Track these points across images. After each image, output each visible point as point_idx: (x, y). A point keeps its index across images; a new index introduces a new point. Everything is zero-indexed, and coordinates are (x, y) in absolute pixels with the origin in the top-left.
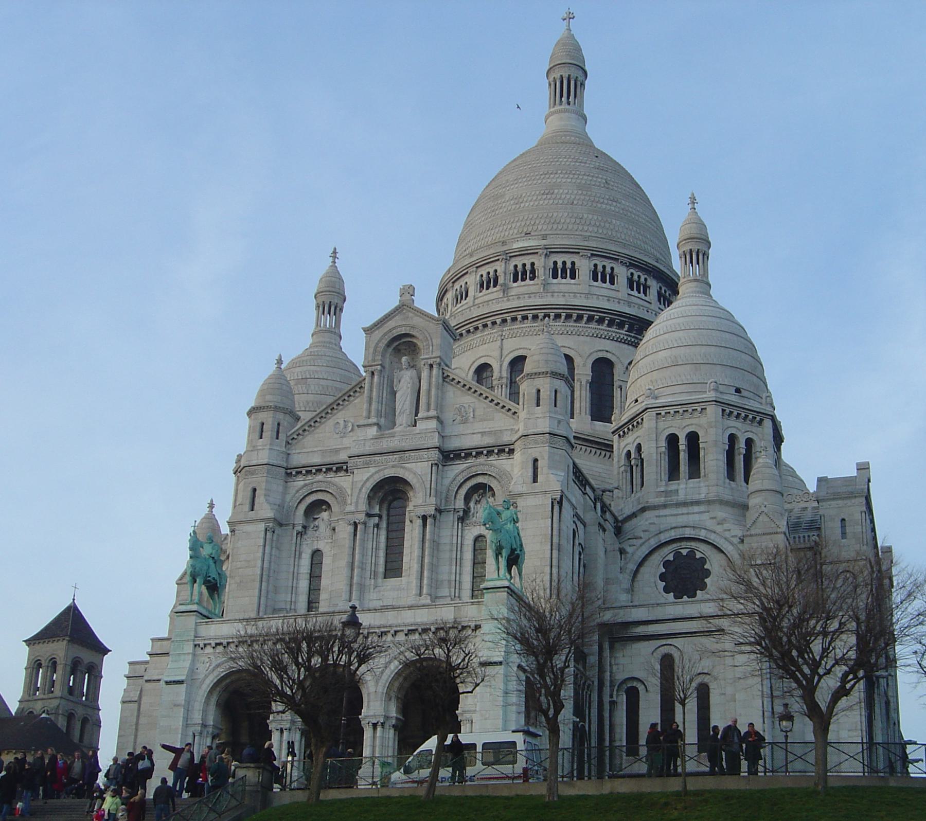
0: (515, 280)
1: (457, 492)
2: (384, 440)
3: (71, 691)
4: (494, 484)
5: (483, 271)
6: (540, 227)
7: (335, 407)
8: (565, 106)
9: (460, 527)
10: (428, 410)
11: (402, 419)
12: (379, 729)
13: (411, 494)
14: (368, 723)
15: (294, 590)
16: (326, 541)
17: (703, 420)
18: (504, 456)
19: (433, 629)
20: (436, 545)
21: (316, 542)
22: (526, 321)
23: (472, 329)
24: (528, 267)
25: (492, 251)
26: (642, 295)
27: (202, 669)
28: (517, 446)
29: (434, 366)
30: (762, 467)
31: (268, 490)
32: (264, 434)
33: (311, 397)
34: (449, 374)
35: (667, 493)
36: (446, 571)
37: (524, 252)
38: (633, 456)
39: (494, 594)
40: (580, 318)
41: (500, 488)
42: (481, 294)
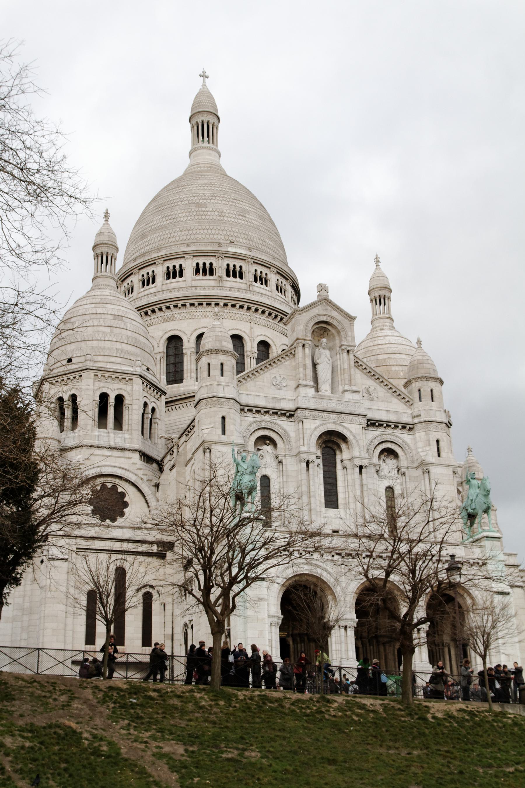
0: (228, 275)
2: (325, 401)
5: (201, 260)
6: (241, 240)
7: (272, 364)
8: (211, 145)
11: (325, 387)
13: (343, 446)
18: (405, 431)
22: (241, 309)
23: (196, 304)
24: (238, 269)
25: (209, 248)
28: (416, 426)
29: (350, 353)
32: (224, 373)
37: (236, 256)
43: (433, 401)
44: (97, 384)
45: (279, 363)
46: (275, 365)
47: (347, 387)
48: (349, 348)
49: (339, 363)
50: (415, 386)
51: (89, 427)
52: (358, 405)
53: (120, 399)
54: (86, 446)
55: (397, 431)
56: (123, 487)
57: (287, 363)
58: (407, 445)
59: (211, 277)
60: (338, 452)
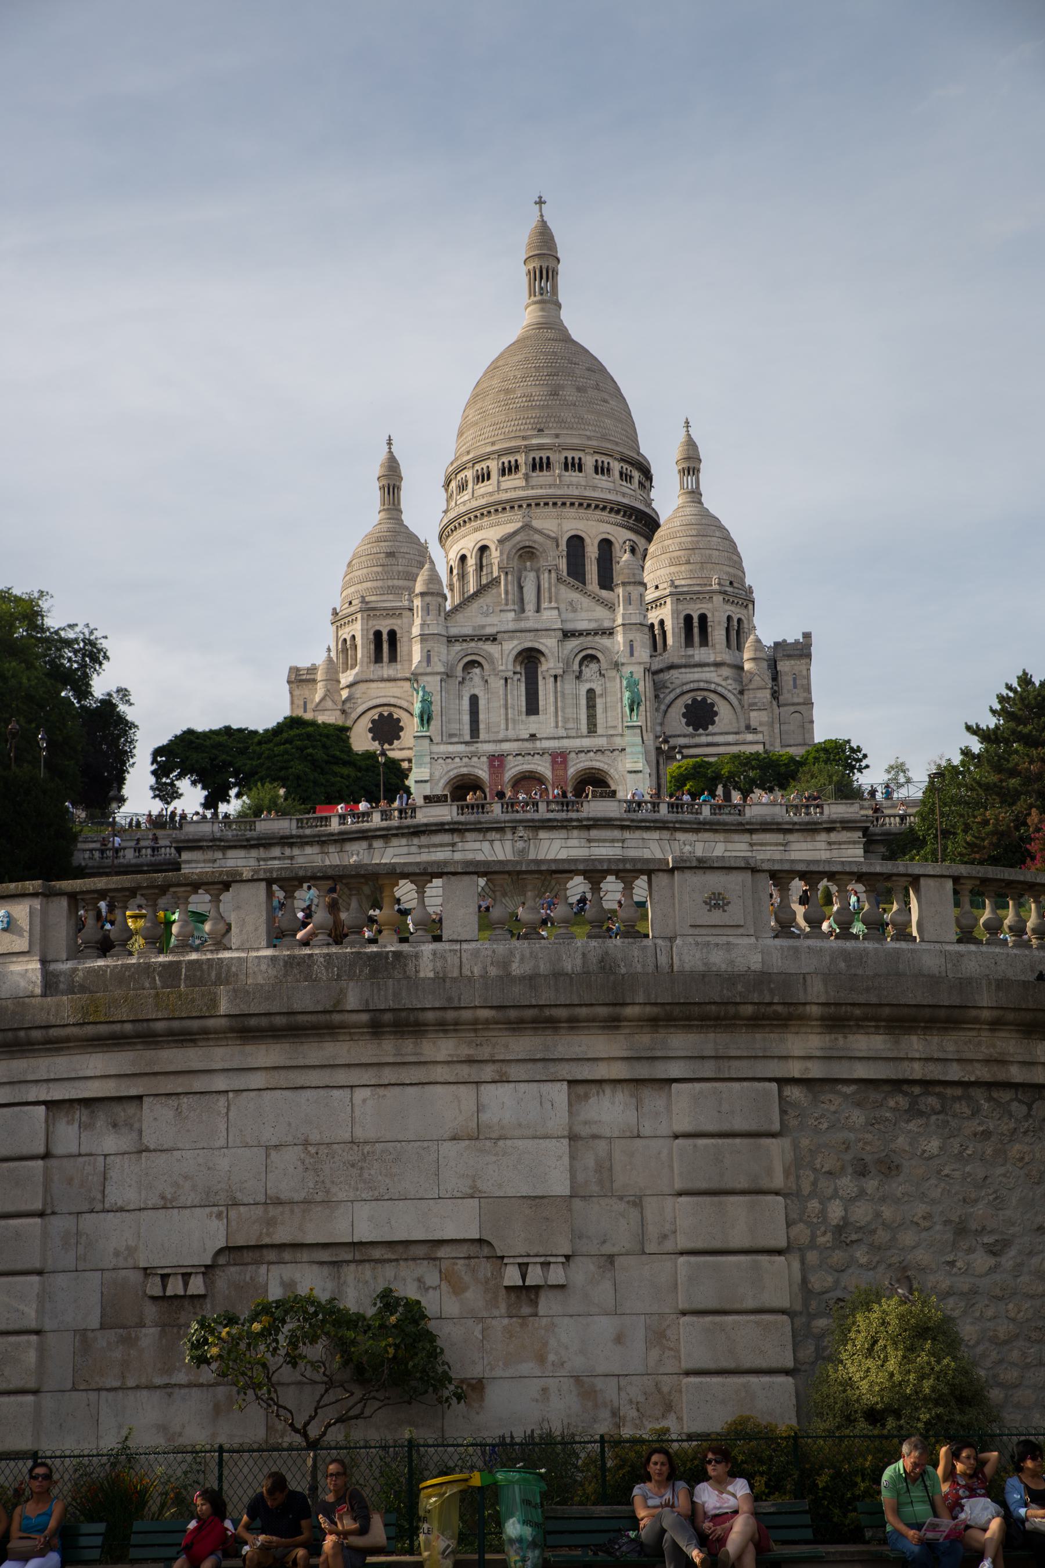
0: (534, 468)
4: (599, 655)
5: (505, 459)
10: (550, 602)
11: (530, 606)
13: (542, 659)
15: (460, 721)
17: (710, 606)
18: (605, 636)
20: (563, 694)
24: (545, 460)
25: (513, 444)
26: (629, 485)
27: (437, 774)
33: (400, 568)
35: (685, 656)
36: (570, 712)
37: (540, 447)
38: (656, 627)
40: (589, 505)
42: (504, 479)
44: (370, 622)
51: (365, 664)
53: (392, 634)
54: (362, 681)
56: (398, 714)
57: (494, 591)
58: (607, 648)
59: (517, 476)
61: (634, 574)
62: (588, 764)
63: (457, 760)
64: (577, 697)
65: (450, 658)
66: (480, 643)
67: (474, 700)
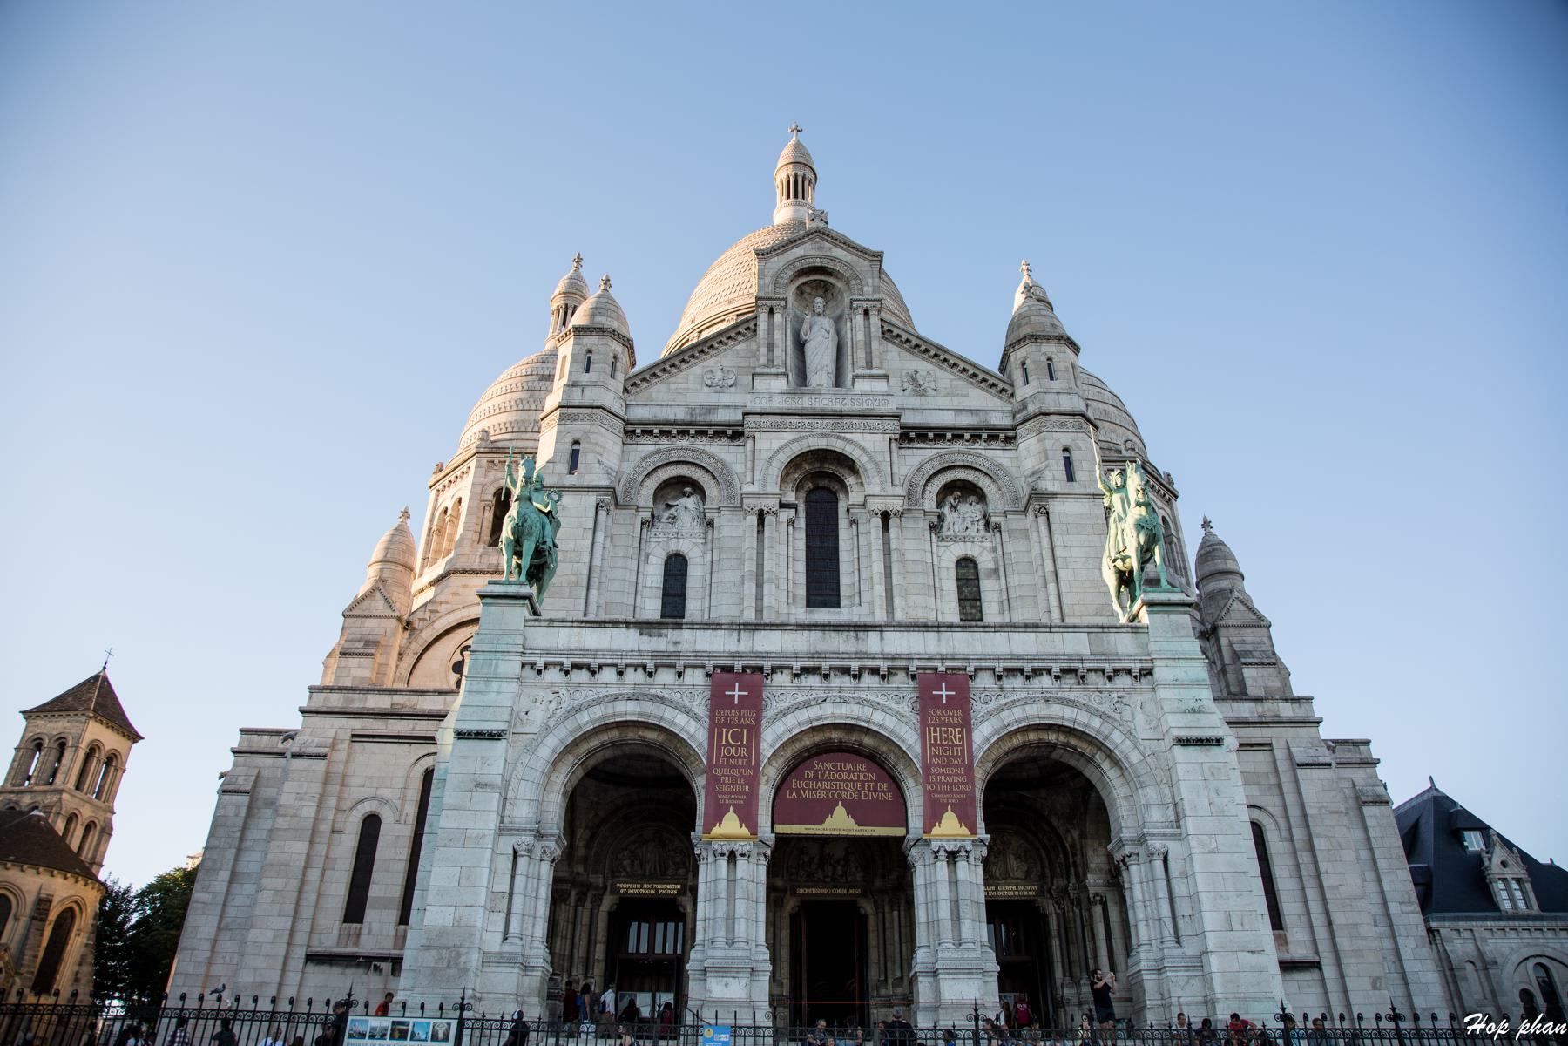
1: (924, 489)
3: (78, 787)
4: (984, 483)
7: (706, 350)
8: (800, 199)
9: (934, 540)
12: (962, 864)
13: (851, 481)
14: (938, 851)
16: (693, 540)
18: (997, 445)
19: (1056, 669)
20: (904, 562)
21: (673, 541)
28: (1021, 430)
29: (871, 313)
30: (1218, 544)
31: (601, 446)
34: (892, 328)
39: (1166, 616)
41: (995, 489)
43: (1052, 379)
44: (492, 474)
45: (721, 347)
46: (713, 352)
47: (858, 371)
48: (865, 305)
49: (849, 336)
50: (1017, 356)
51: (467, 543)
52: (881, 398)
54: (455, 571)
55: (979, 447)
57: (738, 347)
58: (1002, 469)
60: (841, 496)
61: (1053, 325)
62: (1037, 713)
63: (608, 675)
64: (933, 570)
65: (627, 467)
66: (701, 442)
67: (676, 567)
